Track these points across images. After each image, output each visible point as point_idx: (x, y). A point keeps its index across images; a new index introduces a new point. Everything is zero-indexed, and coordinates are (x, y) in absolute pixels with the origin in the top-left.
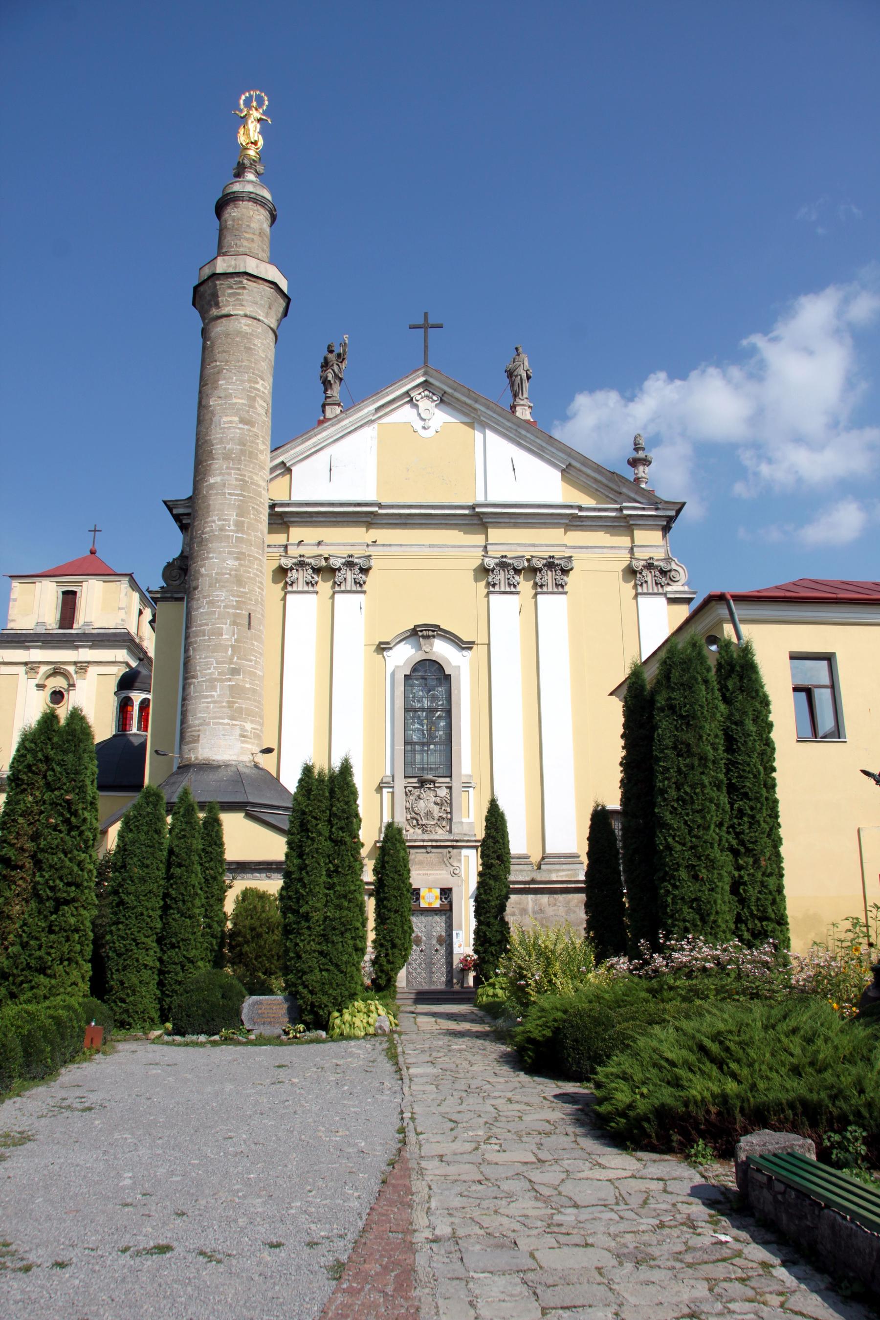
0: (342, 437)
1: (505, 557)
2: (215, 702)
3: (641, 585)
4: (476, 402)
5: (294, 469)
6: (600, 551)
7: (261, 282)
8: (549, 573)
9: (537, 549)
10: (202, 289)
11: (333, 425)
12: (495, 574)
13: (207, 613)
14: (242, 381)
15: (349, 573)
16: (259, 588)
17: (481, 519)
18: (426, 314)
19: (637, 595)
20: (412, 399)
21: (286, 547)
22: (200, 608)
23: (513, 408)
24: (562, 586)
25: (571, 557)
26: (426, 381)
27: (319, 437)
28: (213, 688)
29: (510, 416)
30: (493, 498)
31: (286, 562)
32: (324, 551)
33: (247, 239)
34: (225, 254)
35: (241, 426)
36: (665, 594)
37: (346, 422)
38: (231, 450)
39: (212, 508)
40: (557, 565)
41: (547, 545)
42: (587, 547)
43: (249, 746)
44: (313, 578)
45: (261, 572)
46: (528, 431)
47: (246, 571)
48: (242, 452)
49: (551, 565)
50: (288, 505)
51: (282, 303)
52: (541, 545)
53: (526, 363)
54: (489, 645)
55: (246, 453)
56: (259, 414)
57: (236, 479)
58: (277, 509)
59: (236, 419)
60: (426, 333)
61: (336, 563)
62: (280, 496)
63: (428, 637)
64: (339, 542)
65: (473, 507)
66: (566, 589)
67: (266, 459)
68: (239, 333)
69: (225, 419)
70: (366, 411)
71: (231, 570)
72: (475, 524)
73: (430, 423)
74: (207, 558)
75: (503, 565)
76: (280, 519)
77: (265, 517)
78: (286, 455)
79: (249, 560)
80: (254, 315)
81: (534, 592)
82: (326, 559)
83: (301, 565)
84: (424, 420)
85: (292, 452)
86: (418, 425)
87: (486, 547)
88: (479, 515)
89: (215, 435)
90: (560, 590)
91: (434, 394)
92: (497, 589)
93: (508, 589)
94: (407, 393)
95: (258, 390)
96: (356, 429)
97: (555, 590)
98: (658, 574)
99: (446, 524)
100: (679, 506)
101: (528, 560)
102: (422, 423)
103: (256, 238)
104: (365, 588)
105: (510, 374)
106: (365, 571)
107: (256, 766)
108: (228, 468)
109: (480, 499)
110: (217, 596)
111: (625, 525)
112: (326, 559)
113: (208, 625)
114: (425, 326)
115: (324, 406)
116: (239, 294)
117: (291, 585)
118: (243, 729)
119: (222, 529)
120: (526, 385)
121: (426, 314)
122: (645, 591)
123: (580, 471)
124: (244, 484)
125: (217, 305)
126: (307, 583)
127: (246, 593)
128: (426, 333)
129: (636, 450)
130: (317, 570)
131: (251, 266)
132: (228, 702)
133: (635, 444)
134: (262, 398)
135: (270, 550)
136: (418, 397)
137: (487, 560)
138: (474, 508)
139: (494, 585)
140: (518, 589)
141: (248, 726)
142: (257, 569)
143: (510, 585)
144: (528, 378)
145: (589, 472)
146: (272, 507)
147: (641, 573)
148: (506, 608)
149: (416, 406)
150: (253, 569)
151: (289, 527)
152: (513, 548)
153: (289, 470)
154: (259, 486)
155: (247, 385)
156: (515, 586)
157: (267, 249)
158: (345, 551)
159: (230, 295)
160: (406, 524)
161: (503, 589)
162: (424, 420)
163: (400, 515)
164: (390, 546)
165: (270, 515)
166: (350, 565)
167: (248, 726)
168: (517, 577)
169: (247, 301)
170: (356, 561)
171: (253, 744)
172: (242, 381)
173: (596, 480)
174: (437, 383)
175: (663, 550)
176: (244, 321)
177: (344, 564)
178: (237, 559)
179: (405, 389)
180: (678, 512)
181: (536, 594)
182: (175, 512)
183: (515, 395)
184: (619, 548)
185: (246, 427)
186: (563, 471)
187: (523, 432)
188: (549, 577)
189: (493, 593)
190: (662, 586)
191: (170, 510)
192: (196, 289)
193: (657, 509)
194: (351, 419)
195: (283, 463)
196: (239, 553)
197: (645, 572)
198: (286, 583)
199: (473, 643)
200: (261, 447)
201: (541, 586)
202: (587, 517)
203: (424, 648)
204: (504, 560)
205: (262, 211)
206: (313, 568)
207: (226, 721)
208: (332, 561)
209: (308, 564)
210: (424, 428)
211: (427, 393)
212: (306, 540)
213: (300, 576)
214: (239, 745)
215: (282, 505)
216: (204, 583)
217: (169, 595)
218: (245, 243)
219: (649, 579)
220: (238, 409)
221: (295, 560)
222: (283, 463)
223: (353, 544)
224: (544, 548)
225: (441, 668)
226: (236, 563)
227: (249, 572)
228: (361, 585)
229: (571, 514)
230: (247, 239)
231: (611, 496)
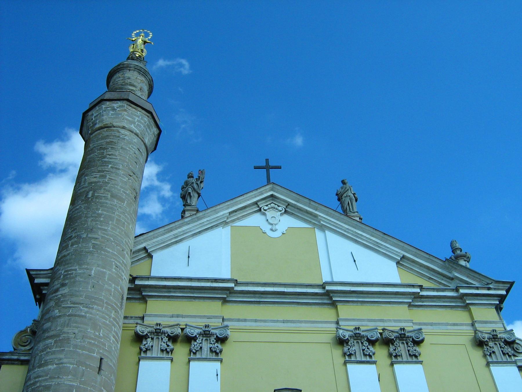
0: (200, 232)
3: (490, 355)
4: (316, 210)
5: (155, 255)
6: (444, 327)
7: (140, 109)
8: (402, 345)
9: (386, 324)
10: (90, 113)
12: (352, 345)
16: (114, 337)
17: (331, 298)
18: (267, 160)
19: (488, 364)
20: (260, 210)
21: (143, 318)
24: (416, 357)
25: (421, 329)
26: (272, 196)
32: (183, 322)
36: (515, 362)
37: (205, 220)
40: (408, 337)
41: (395, 321)
44: (168, 346)
45: (118, 323)
46: (363, 232)
49: (402, 336)
50: (148, 278)
52: (390, 321)
58: (137, 282)
64: (194, 315)
65: (323, 286)
66: (420, 359)
70: (221, 213)
75: (357, 336)
78: (149, 242)
79: (106, 308)
83: (158, 332)
84: (272, 224)
85: (154, 240)
86: (266, 228)
87: (337, 323)
88: (328, 294)
90: (414, 359)
91: (279, 206)
92: (353, 358)
93: (364, 359)
94: (256, 203)
97: (410, 359)
98: (502, 344)
99: (298, 303)
100: (509, 285)
102: (270, 227)
104: (220, 357)
106: (222, 340)
112: (182, 329)
117: (145, 352)
121: (267, 160)
122: (495, 360)
123: (414, 261)
126: (162, 351)
127: (99, 337)
129: (453, 252)
130: (174, 339)
133: (452, 248)
135: (126, 321)
136: (266, 208)
137: (341, 332)
138: (324, 288)
139: (350, 355)
140: (373, 359)
142: (114, 319)
143: (365, 355)
146: (133, 280)
147: (487, 345)
150: (110, 317)
153: (150, 256)
156: (370, 356)
158: (201, 323)
160: (259, 303)
161: (359, 359)
162: (272, 224)
164: (245, 320)
165: (129, 289)
166: (206, 334)
168: (371, 348)
169: (127, 119)
173: (428, 268)
176: (123, 131)
177: (200, 334)
179: (255, 200)
180: (508, 291)
181: (392, 364)
182: (37, 281)
184: (462, 325)
186: (398, 263)
188: (402, 348)
190: (510, 356)
192: (85, 114)
193: (489, 289)
194: (208, 219)
195: (145, 249)
197: (491, 344)
198: (141, 349)
201: (396, 356)
204: (357, 332)
205: (144, 79)
209: (164, 333)
210: (272, 230)
211: (272, 205)
212: (161, 313)
213: (156, 345)
217: (16, 357)
219: (496, 349)
221: (149, 329)
222: (145, 249)
224: (394, 324)
227: (106, 319)
228: (217, 354)
229: (414, 293)
231: (443, 282)
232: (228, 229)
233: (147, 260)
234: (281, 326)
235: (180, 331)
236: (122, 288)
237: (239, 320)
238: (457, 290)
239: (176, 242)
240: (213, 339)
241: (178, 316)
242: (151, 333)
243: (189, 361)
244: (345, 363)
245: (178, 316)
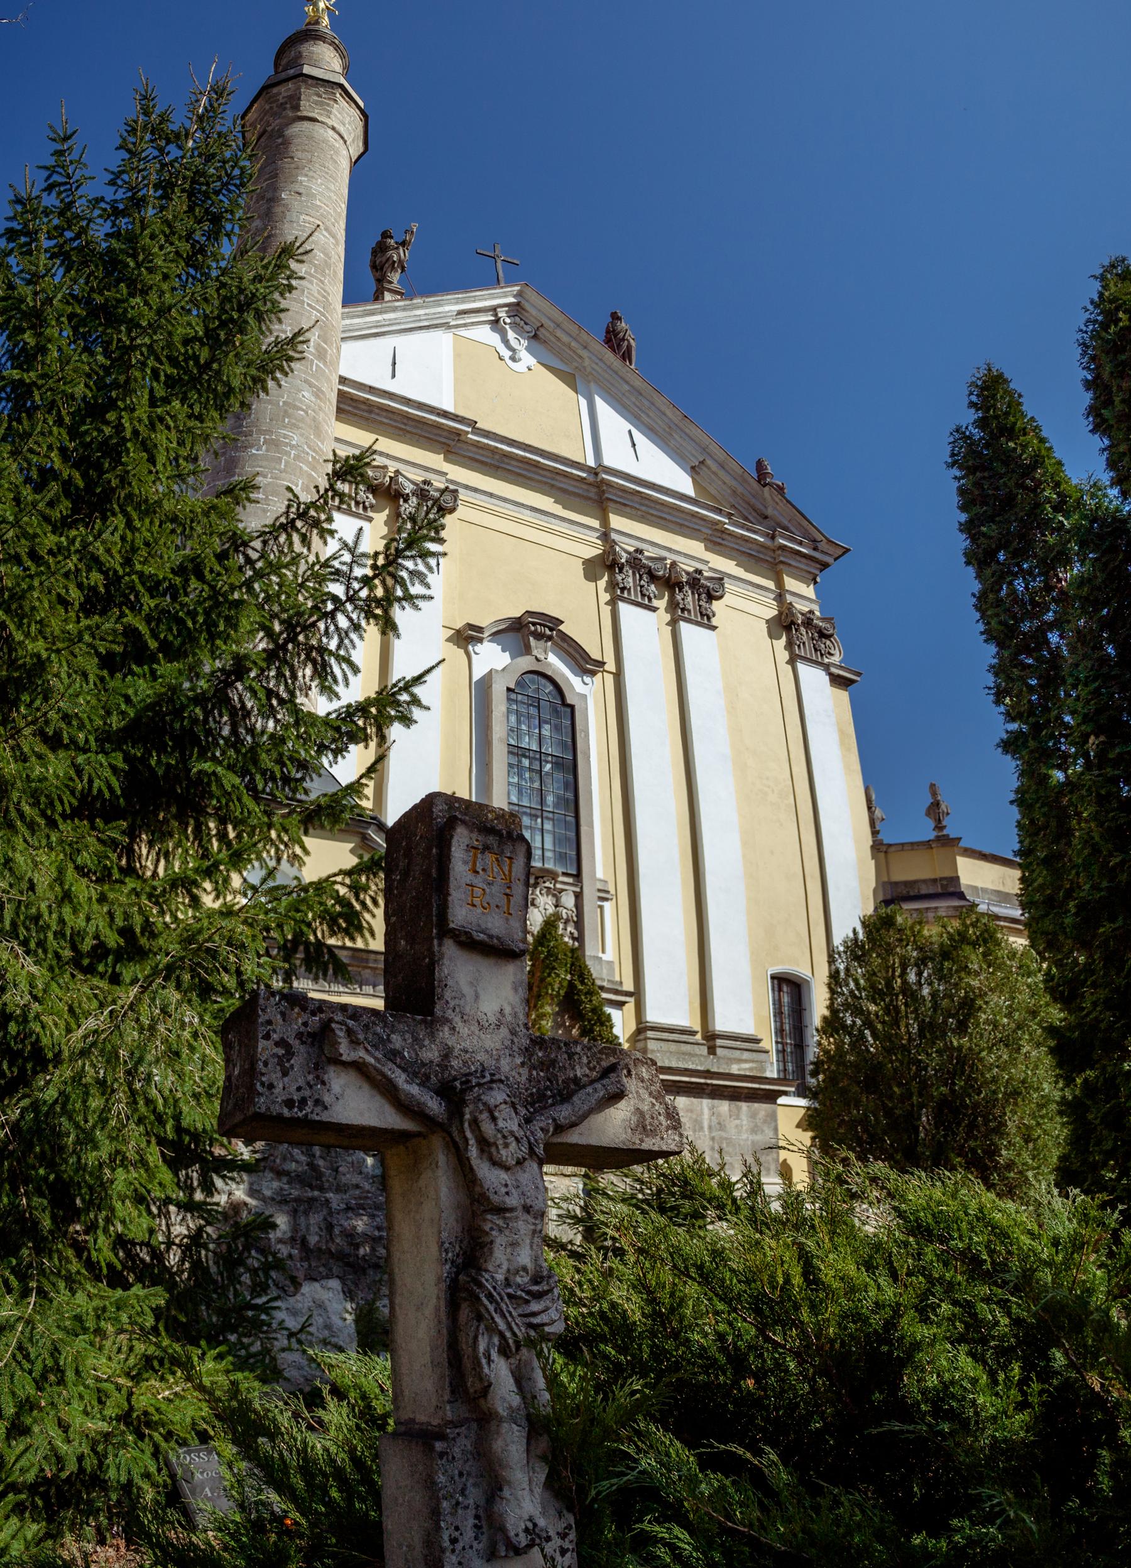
8: (689, 597)
13: (265, 458)
22: (252, 447)
49: (695, 581)
65: (595, 472)
68: (325, 141)
72: (590, 499)
94: (494, 309)
110: (285, 436)
113: (265, 477)
156: (650, 599)
174: (534, 312)
176: (331, 132)
188: (689, 599)
189: (624, 600)
234: (527, 515)
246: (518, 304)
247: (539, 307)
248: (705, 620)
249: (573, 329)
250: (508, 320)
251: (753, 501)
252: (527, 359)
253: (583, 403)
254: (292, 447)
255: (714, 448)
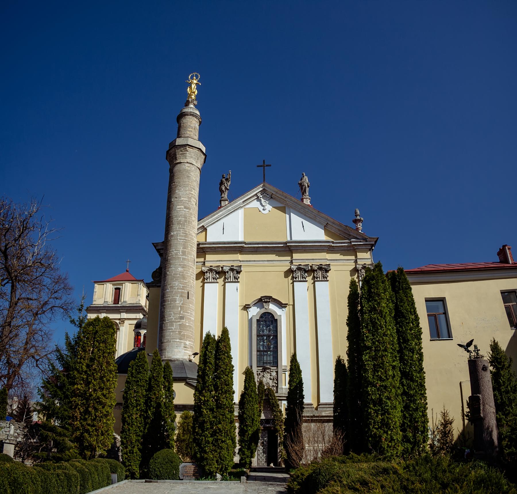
1: (301, 265)
2: (172, 332)
5: (208, 229)
9: (314, 261)
11: (224, 209)
14: (186, 190)
15: (232, 274)
18: (264, 161)
21: (204, 262)
23: (302, 200)
27: (219, 214)
28: (172, 325)
29: (301, 203)
30: (294, 239)
31: (205, 269)
32: (221, 264)
33: (189, 131)
34: (180, 137)
35: (185, 210)
37: (230, 208)
38: (180, 220)
39: (172, 245)
42: (336, 260)
43: (188, 352)
47: (186, 273)
48: (185, 221)
49: (320, 268)
50: (205, 244)
51: (203, 157)
53: (307, 180)
54: (294, 305)
55: (187, 221)
56: (193, 205)
57: (183, 233)
59: (183, 207)
60: (264, 168)
61: (226, 269)
62: (202, 240)
63: (266, 302)
65: (286, 243)
66: (328, 279)
67: (195, 224)
69: (178, 207)
70: (239, 203)
71: (180, 272)
73: (266, 207)
74: (170, 267)
75: (299, 269)
76: (203, 250)
77: (195, 249)
80: (191, 162)
81: (313, 281)
82: (222, 268)
83: (211, 270)
84: (263, 206)
85: (207, 221)
86: (261, 208)
89: (174, 213)
92: (297, 280)
94: (256, 195)
95: (192, 194)
96: (234, 211)
101: (311, 266)
103: (193, 130)
104: (239, 280)
105: (301, 185)
106: (239, 272)
107: (190, 361)
108: (179, 228)
109: (289, 239)
110: (174, 284)
111: (352, 250)
114: (264, 166)
115: (221, 201)
116: (185, 154)
118: (185, 344)
119: (176, 254)
120: (307, 189)
121: (264, 161)
124: (186, 235)
125: (176, 158)
126: (214, 279)
128: (264, 168)
130: (218, 273)
131: (190, 142)
132: (179, 332)
134: (194, 198)
135: (198, 264)
137: (292, 266)
139: (296, 278)
141: (188, 343)
143: (303, 278)
144: (308, 186)
145: (336, 226)
146: (198, 245)
148: (302, 289)
149: (261, 200)
151: (206, 254)
152: (304, 261)
154: (193, 236)
155: (188, 192)
156: (305, 278)
157: (197, 135)
158: (230, 264)
159: (181, 154)
162: (263, 206)
163: (254, 247)
164: (250, 261)
165: (197, 248)
166: (232, 270)
167: (188, 343)
168: (306, 274)
170: (235, 268)
171: (189, 351)
172: (186, 190)
174: (269, 190)
175: (370, 260)
176: (187, 165)
177: (229, 270)
178: (183, 267)
183: (303, 194)
185: (187, 210)
187: (307, 210)
188: (320, 274)
189: (296, 281)
191: (155, 247)
196: (183, 265)
199: (287, 304)
200: (193, 219)
202: (336, 246)
203: (265, 307)
206: (216, 272)
207: (178, 340)
208: (224, 268)
209: (214, 270)
210: (264, 210)
212: (213, 260)
214: (184, 351)
215: (203, 244)
216: (169, 278)
218: (188, 132)
220: (184, 203)
223: (234, 261)
224: (318, 261)
225: (273, 316)
226: (182, 269)
228: (237, 279)
230: (189, 131)
232: (243, 209)
233: (204, 233)
235: (221, 269)
236: (194, 256)
237: (247, 261)
238: (351, 242)
239: (217, 221)
240: (235, 272)
241: (220, 261)
242: (208, 270)
243: (225, 283)
244: (293, 283)
245: (220, 261)
246: (264, 189)
247: (271, 189)
248: (325, 279)
249: (281, 193)
250: (261, 196)
251: (345, 231)
252: (269, 207)
253: (287, 216)
254: (176, 286)
255: (329, 218)
